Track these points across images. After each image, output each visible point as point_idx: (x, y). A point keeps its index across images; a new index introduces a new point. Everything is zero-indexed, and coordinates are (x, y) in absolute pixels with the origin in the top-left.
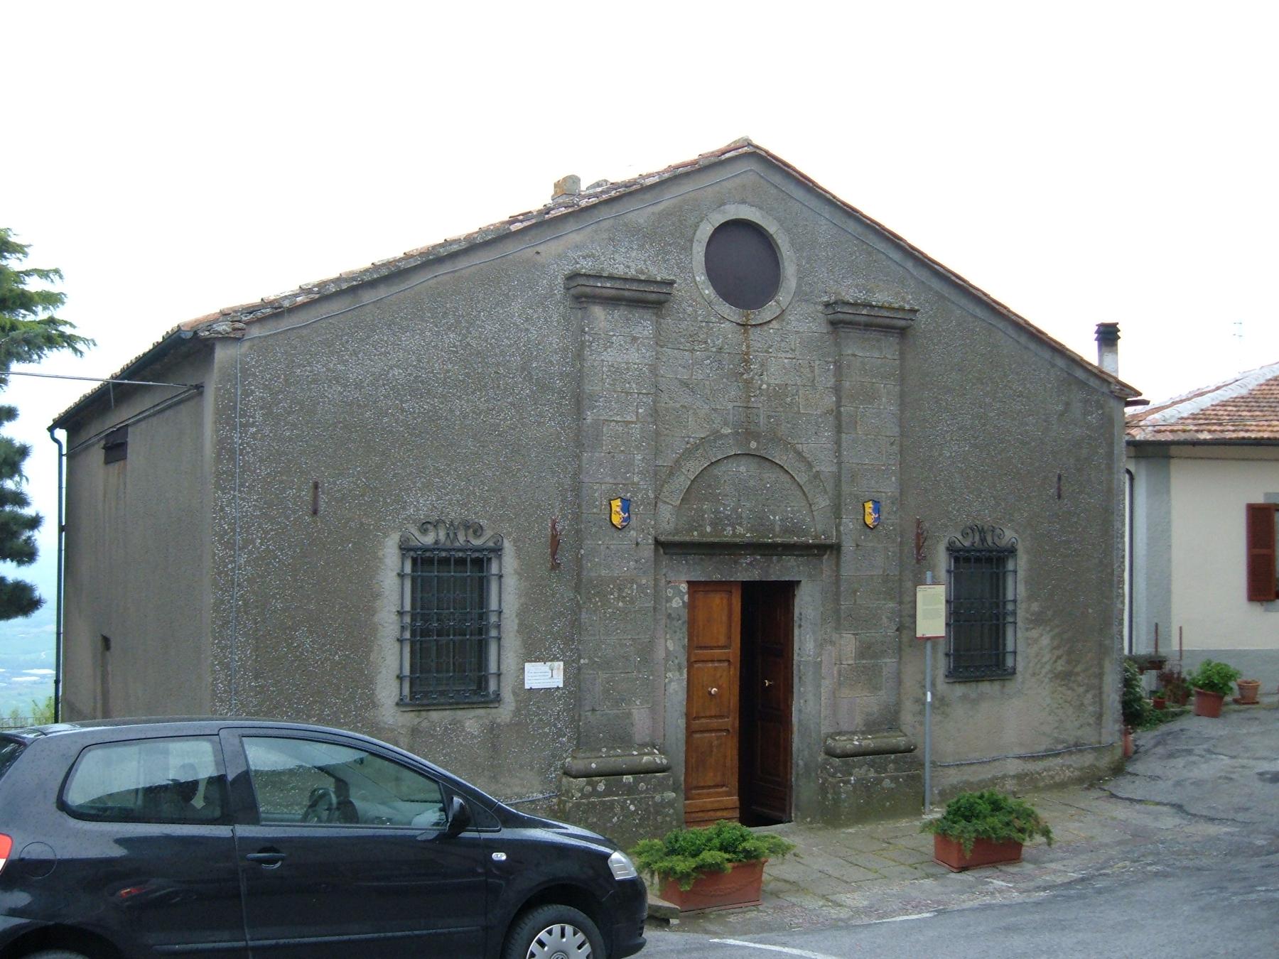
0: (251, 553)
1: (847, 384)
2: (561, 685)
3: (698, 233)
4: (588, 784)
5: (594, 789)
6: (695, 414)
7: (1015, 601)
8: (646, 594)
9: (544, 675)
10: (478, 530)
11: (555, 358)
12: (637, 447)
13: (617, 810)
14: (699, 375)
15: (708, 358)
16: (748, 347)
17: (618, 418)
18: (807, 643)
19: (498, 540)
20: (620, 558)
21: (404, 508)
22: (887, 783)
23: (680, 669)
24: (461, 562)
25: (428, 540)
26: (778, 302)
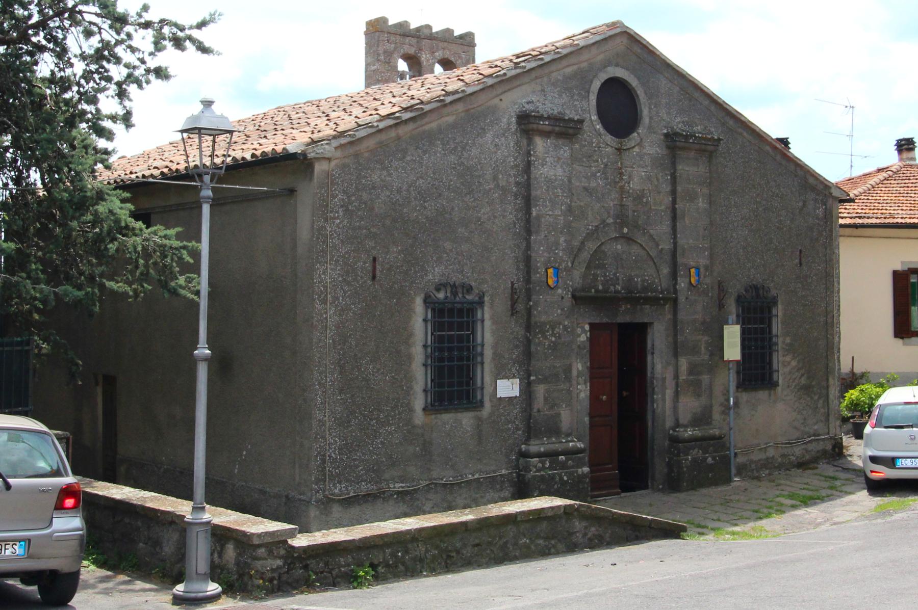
1: (679, 189)
4: (540, 462)
5: (543, 466)
9: (508, 388)
10: (469, 289)
11: (512, 172)
12: (561, 233)
14: (593, 184)
15: (599, 171)
17: (550, 213)
18: (659, 364)
19: (481, 297)
20: (552, 306)
21: (426, 275)
22: (710, 460)
23: (585, 383)
25: (441, 295)
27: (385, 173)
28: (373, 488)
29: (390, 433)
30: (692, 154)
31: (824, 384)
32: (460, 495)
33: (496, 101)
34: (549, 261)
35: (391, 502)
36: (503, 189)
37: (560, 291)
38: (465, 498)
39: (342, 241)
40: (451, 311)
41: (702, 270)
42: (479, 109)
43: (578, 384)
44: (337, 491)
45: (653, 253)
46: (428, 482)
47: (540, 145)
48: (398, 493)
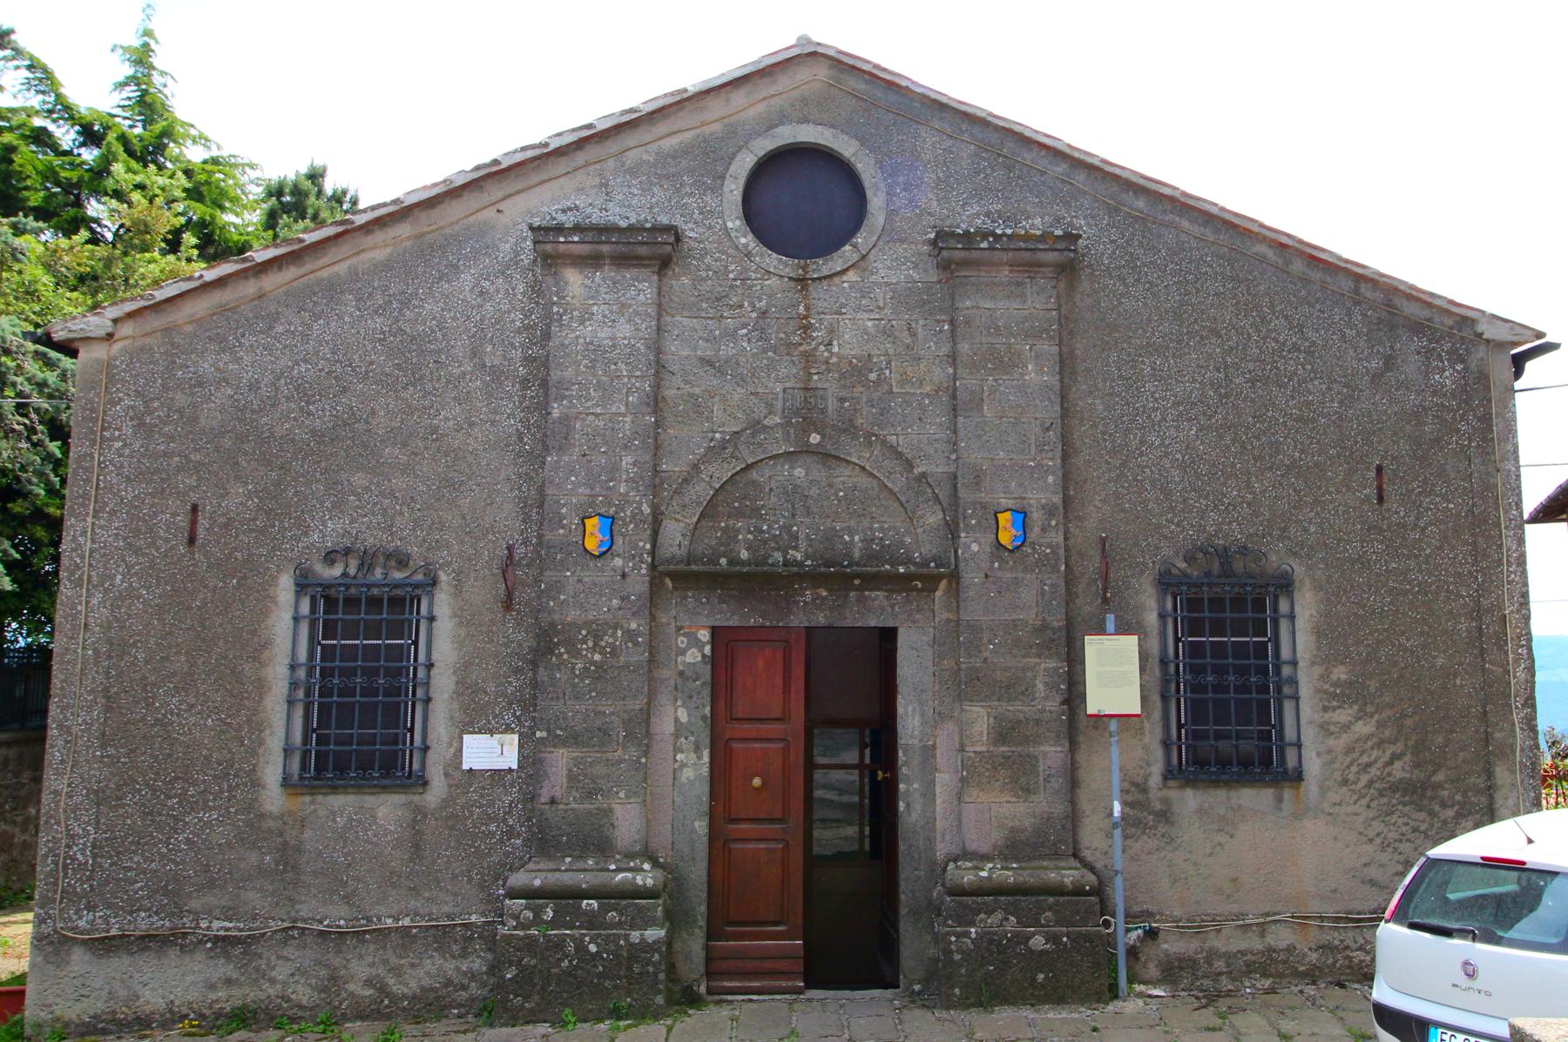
0: (106, 591)
2: (515, 766)
3: (732, 168)
4: (527, 908)
6: (724, 400)
7: (1294, 663)
8: (636, 644)
9: (490, 752)
10: (403, 562)
11: (517, 341)
12: (626, 447)
13: (571, 947)
14: (728, 350)
15: (744, 326)
16: (807, 308)
17: (599, 410)
21: (306, 534)
23: (697, 749)
24: (375, 603)
26: (855, 246)
27: (226, 357)
28: (163, 924)
29: (208, 824)
30: (1005, 274)
31: (1481, 782)
32: (361, 957)
33: (489, 213)
34: (592, 504)
35: (199, 956)
36: (497, 374)
37: (618, 562)
38: (372, 965)
39: (128, 479)
40: (352, 603)
41: (1036, 515)
42: (446, 231)
43: (677, 750)
44: (82, 923)
45: (897, 483)
46: (286, 924)
47: (575, 281)
48: (216, 939)
